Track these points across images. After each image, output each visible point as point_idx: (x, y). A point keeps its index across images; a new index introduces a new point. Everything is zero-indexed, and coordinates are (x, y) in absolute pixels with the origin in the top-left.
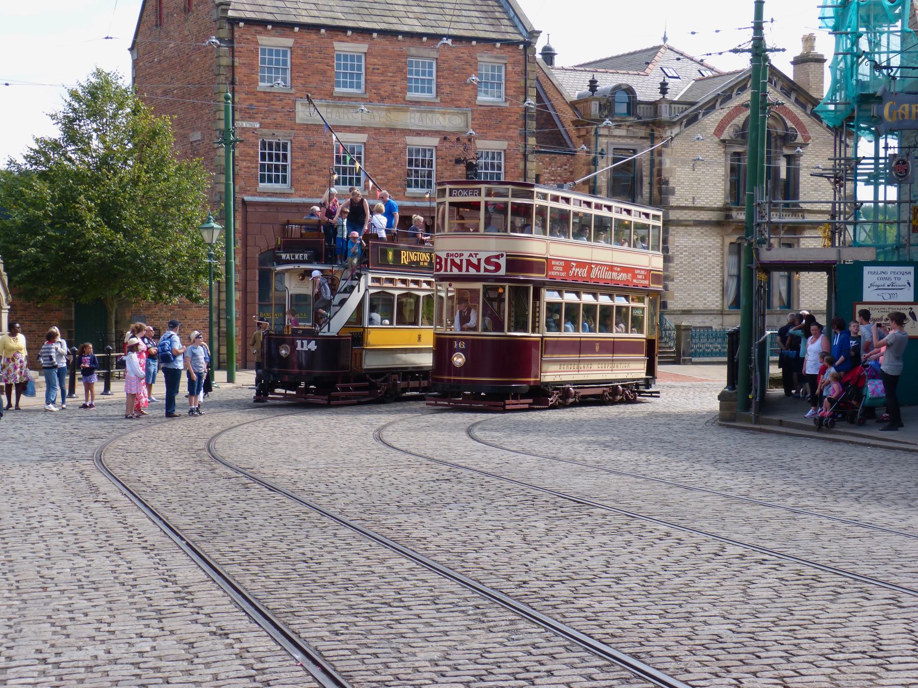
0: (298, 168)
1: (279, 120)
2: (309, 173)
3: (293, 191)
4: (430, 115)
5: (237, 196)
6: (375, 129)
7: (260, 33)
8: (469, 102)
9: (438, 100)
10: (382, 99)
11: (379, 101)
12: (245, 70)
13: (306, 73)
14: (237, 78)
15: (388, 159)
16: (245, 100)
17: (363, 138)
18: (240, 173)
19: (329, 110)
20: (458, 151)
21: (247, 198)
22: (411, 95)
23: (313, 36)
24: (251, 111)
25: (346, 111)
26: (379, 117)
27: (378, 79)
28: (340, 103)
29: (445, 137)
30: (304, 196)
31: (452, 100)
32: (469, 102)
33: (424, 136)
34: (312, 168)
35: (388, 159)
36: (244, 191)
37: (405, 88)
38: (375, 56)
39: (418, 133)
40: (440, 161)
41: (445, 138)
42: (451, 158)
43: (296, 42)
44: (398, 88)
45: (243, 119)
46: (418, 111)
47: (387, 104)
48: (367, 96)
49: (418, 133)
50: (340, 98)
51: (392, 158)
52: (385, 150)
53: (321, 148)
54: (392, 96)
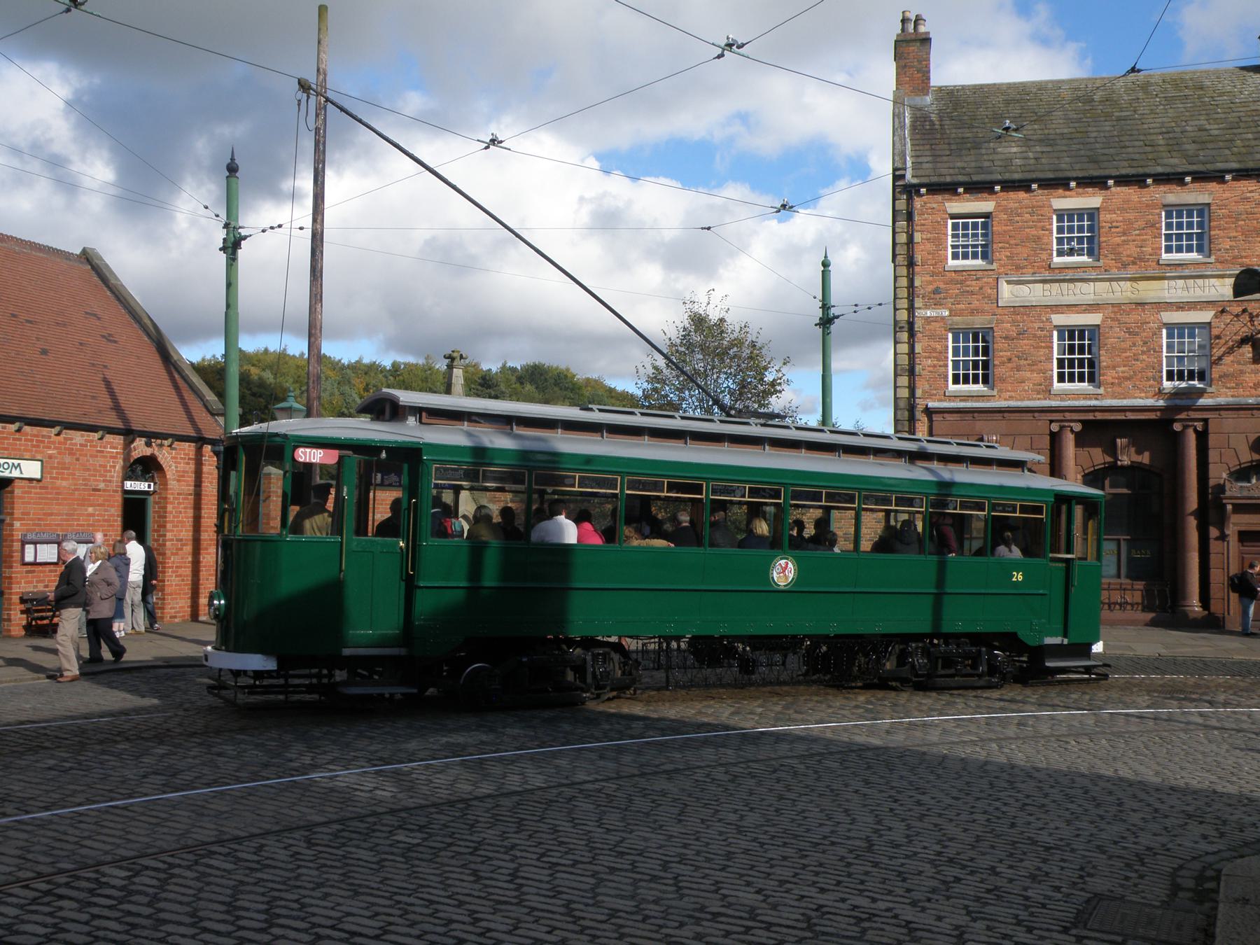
0: (1003, 363)
1: (976, 304)
2: (1018, 369)
3: (995, 393)
5: (921, 404)
7: (950, 200)
10: (1125, 266)
11: (1119, 269)
12: (930, 247)
13: (1012, 242)
14: (918, 258)
15: (1134, 345)
16: (930, 283)
18: (923, 373)
19: (1047, 286)
21: (931, 405)
23: (1022, 195)
24: (938, 296)
25: (1071, 286)
26: (1123, 291)
27: (1118, 240)
30: (1011, 398)
31: (1235, 258)
33: (1189, 310)
34: (1022, 362)
35: (1134, 345)
36: (929, 395)
38: (1113, 211)
39: (1180, 306)
43: (998, 205)
45: (927, 307)
47: (1131, 271)
49: (1180, 306)
50: (1062, 269)
52: (1130, 333)
53: (1035, 336)
54: (1138, 260)
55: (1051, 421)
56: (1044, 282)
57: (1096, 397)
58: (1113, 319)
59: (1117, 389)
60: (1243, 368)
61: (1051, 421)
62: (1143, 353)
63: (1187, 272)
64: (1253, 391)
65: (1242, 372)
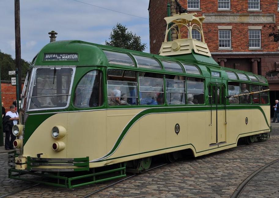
4: (258, 17)
6: (235, 23)
8: (274, 11)
9: (261, 11)
10: (238, 12)
11: (236, 12)
15: (241, 36)
17: (230, 27)
19: (216, 17)
20: (270, 31)
22: (250, 10)
25: (223, 17)
28: (220, 14)
29: (264, 25)
31: (267, 10)
32: (274, 11)
33: (256, 25)
37: (247, 7)
39: (253, 24)
40: (263, 35)
41: (264, 26)
42: (267, 34)
44: (244, 7)
46: (253, 16)
47: (239, 14)
48: (231, 11)
49: (253, 24)
51: (243, 35)
53: (213, 32)
54: (242, 10)
55: (218, 59)
56: (215, 16)
57: (231, 51)
58: (235, 28)
59: (236, 49)
60: (270, 43)
61: (218, 59)
62: (244, 38)
63: (255, 14)
64: (272, 50)
65: (269, 44)
